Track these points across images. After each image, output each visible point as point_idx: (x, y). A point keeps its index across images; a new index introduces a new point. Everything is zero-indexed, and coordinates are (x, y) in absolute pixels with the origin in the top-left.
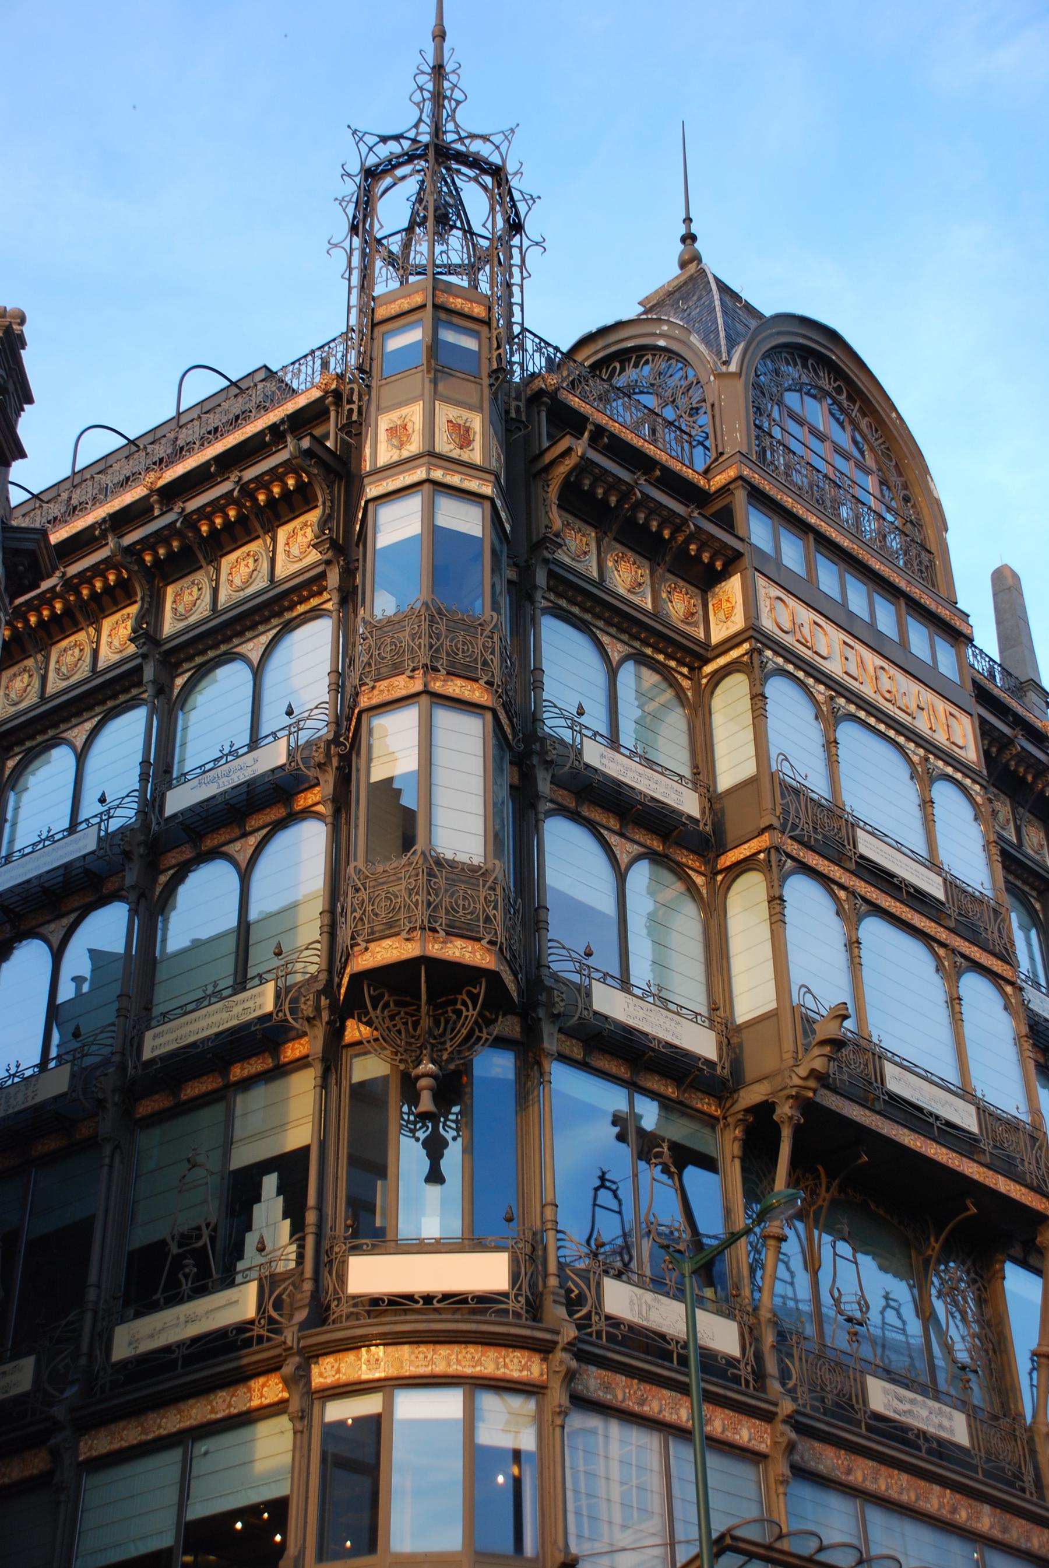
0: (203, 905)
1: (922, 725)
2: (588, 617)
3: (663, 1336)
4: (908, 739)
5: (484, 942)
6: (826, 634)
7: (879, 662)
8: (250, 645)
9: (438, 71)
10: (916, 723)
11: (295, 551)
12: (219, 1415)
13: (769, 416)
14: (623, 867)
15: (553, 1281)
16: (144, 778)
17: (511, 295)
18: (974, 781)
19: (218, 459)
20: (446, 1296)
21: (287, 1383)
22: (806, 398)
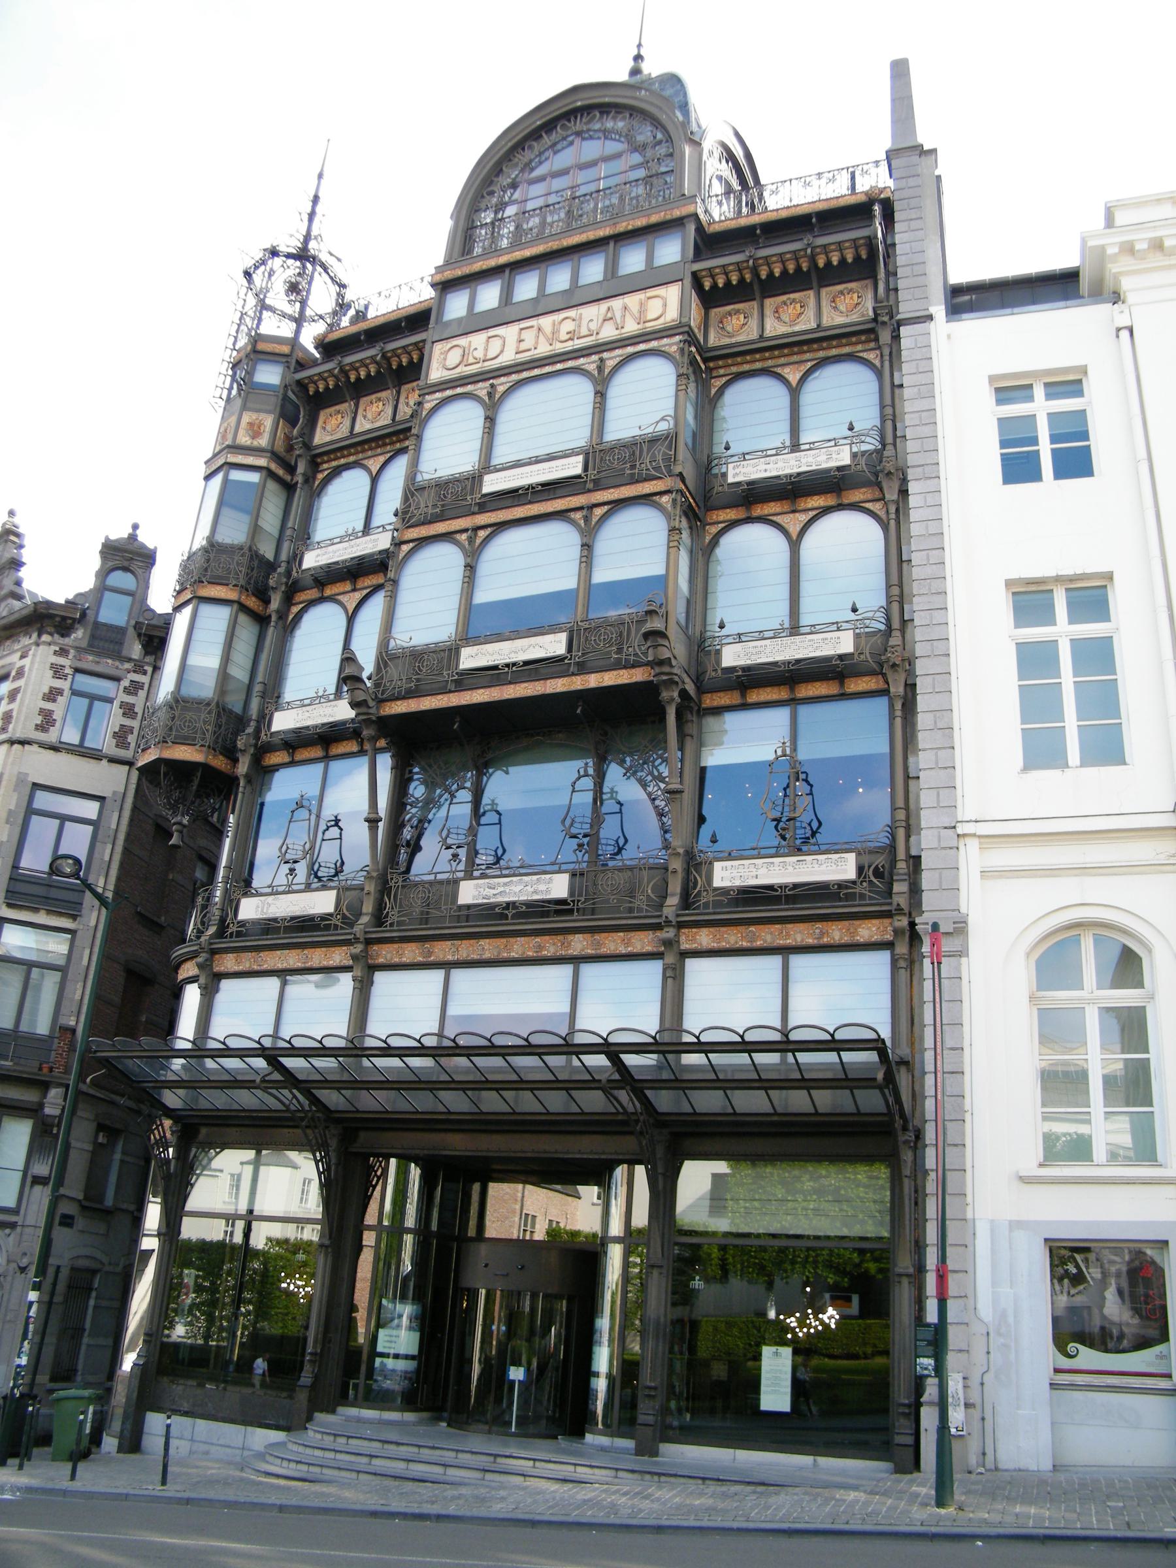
1: (609, 333)
3: (275, 920)
9: (316, 199)
10: (600, 336)
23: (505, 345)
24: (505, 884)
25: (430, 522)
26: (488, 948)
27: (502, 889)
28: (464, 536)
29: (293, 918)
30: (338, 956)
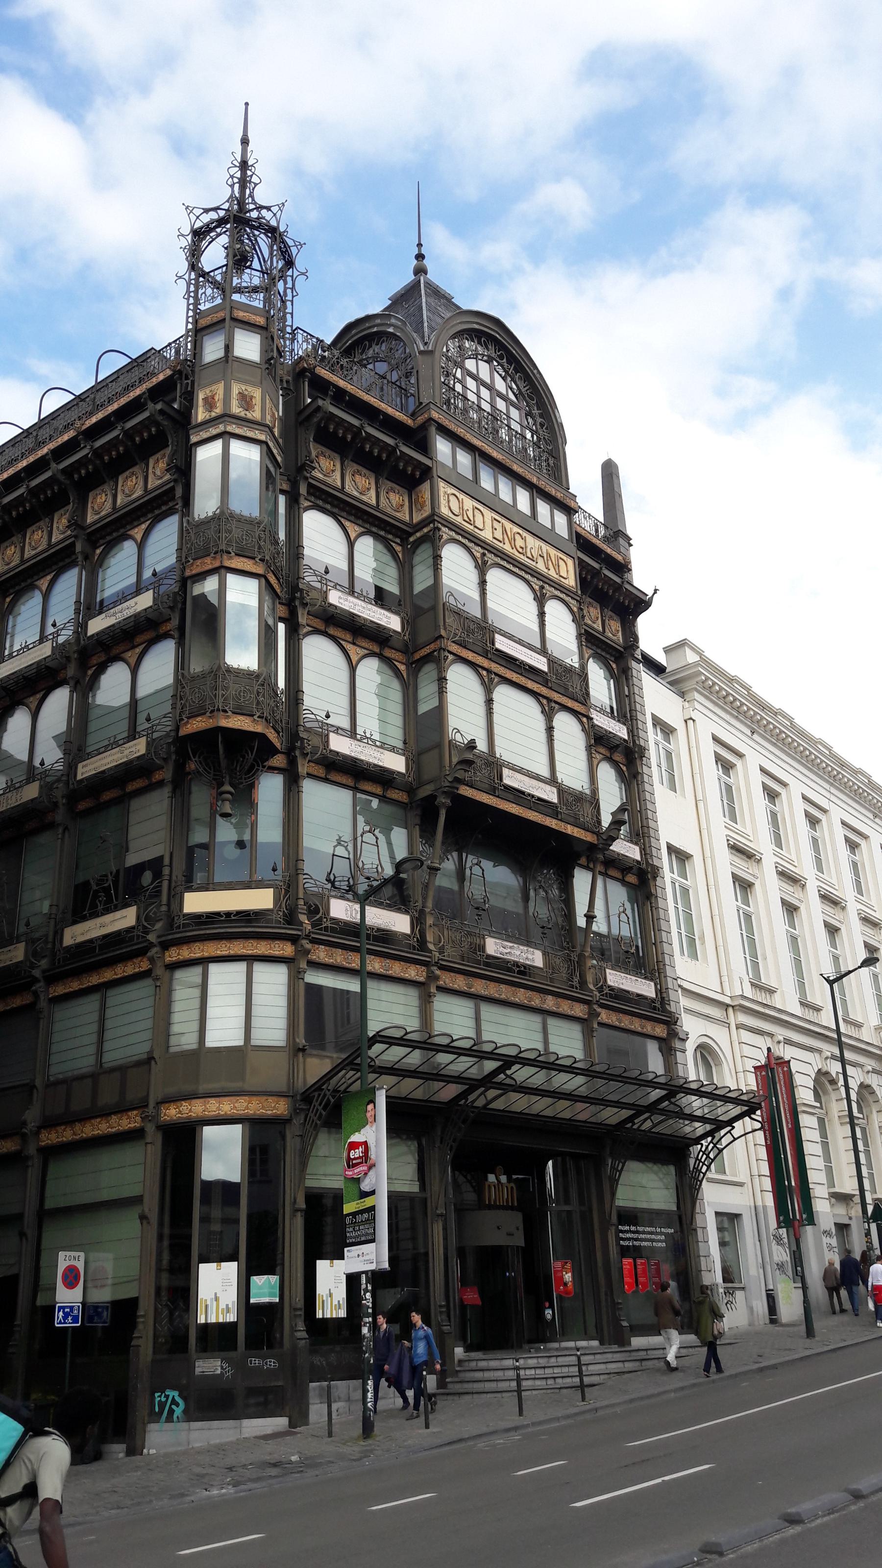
0: (113, 687)
1: (541, 566)
2: (335, 510)
4: (532, 576)
5: (255, 717)
6: (483, 515)
7: (516, 529)
8: (136, 530)
11: (158, 473)
12: (119, 976)
13: (454, 376)
14: (354, 663)
15: (301, 902)
16: (77, 611)
17: (286, 308)
18: (572, 598)
19: (115, 413)
20: (239, 913)
21: (152, 960)
22: (480, 362)
23: (487, 526)
24: (511, 947)
25: (465, 647)
26: (504, 992)
27: (509, 950)
28: (484, 673)
29: (379, 930)
30: (413, 973)
